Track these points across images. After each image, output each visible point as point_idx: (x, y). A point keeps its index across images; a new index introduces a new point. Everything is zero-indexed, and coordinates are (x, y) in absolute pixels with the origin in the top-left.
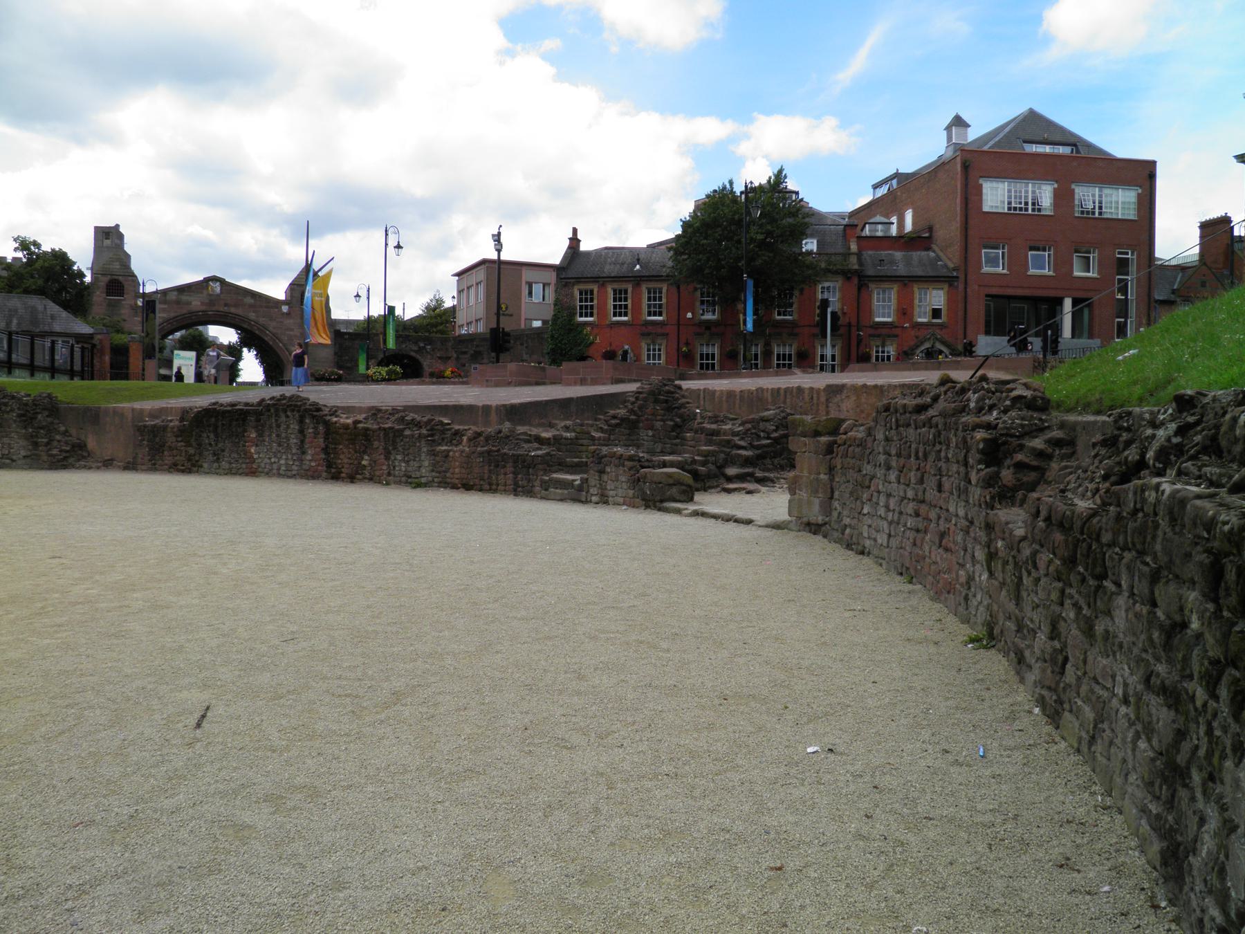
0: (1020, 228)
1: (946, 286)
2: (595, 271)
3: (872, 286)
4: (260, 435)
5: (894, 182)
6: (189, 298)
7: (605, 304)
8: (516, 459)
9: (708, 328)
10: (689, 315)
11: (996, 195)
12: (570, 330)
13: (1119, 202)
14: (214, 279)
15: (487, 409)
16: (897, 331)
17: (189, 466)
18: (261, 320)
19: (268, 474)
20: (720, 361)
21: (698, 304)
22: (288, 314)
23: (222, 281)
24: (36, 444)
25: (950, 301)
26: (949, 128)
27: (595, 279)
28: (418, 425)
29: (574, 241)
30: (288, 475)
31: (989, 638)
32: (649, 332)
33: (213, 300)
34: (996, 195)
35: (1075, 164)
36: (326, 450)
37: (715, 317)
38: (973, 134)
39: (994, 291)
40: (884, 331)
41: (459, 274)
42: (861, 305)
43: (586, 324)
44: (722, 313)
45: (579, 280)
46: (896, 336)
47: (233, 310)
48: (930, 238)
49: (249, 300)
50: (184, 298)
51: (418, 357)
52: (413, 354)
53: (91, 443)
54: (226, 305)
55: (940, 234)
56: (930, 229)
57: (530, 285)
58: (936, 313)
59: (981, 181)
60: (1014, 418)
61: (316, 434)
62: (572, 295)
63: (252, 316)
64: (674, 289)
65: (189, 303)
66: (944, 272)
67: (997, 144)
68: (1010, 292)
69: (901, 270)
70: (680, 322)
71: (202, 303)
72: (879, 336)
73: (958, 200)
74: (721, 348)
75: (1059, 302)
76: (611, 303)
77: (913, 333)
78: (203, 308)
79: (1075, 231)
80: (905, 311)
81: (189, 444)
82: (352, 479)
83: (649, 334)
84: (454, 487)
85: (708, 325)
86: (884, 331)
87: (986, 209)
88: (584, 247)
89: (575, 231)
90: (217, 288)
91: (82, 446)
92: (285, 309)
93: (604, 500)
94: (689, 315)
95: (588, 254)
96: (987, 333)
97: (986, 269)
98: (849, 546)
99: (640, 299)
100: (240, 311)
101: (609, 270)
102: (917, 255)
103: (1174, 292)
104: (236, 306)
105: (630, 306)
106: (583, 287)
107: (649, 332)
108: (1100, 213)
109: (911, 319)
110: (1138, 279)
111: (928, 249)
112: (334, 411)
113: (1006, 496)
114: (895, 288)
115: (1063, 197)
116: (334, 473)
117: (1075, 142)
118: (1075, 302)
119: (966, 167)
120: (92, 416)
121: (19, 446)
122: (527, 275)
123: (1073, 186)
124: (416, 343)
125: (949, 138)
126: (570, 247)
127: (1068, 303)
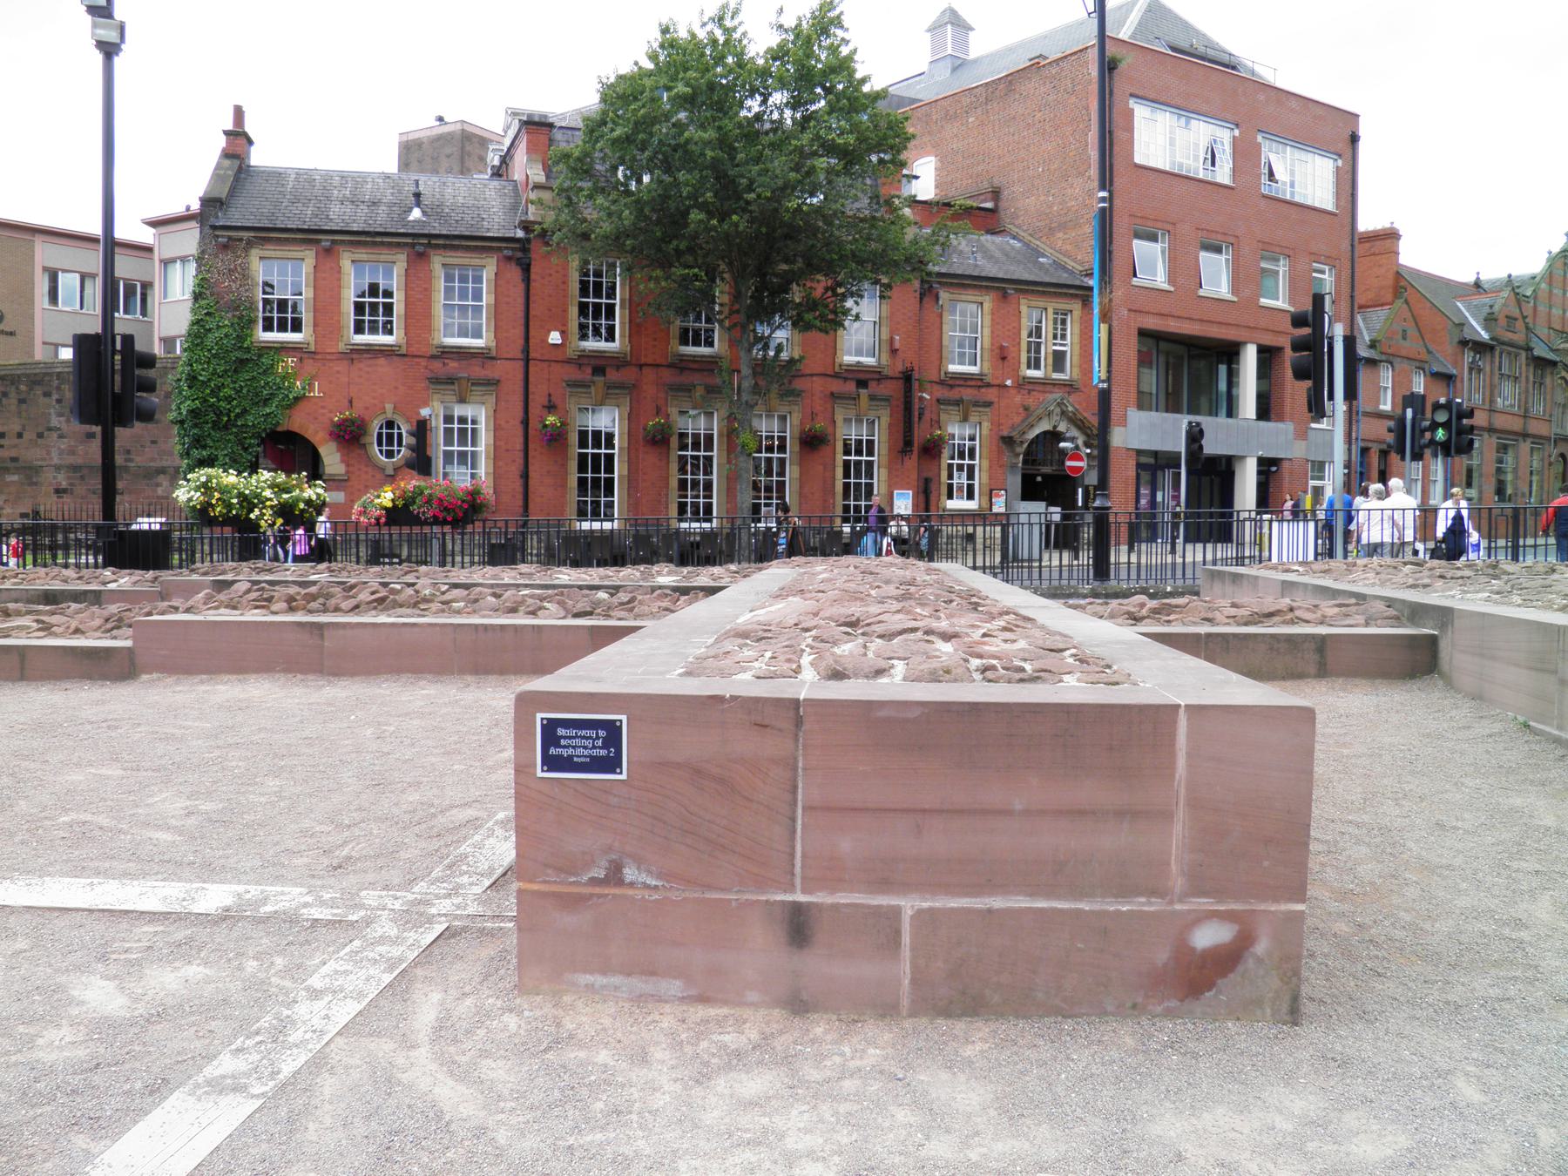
1: (1076, 306)
2: (306, 216)
3: (944, 295)
9: (599, 370)
10: (555, 337)
13: (1306, 177)
16: (991, 394)
21: (574, 311)
26: (935, 28)
27: (308, 236)
29: (238, 138)
32: (454, 372)
35: (1261, 97)
37: (614, 346)
38: (979, 45)
39: (1152, 323)
40: (967, 394)
42: (927, 335)
43: (284, 348)
44: (635, 328)
45: (270, 235)
46: (988, 404)
48: (992, 211)
55: (1024, 204)
56: (996, 194)
57: (53, 277)
59: (1132, 103)
62: (246, 275)
64: (514, 273)
66: (1064, 278)
68: (1173, 326)
69: (992, 270)
72: (957, 403)
73: (1093, 136)
74: (632, 418)
75: (1229, 353)
77: (1018, 399)
80: (1002, 356)
83: (450, 381)
85: (599, 364)
86: (967, 394)
87: (1138, 159)
88: (259, 157)
89: (239, 113)
94: (555, 337)
95: (277, 175)
96: (1140, 407)
99: (428, 292)
101: (339, 215)
102: (987, 239)
103: (1373, 345)
108: (1293, 194)
114: (988, 301)
115: (1245, 155)
119: (1108, 67)
123: (1260, 138)
125: (937, 46)
126: (227, 155)
127: (1250, 357)
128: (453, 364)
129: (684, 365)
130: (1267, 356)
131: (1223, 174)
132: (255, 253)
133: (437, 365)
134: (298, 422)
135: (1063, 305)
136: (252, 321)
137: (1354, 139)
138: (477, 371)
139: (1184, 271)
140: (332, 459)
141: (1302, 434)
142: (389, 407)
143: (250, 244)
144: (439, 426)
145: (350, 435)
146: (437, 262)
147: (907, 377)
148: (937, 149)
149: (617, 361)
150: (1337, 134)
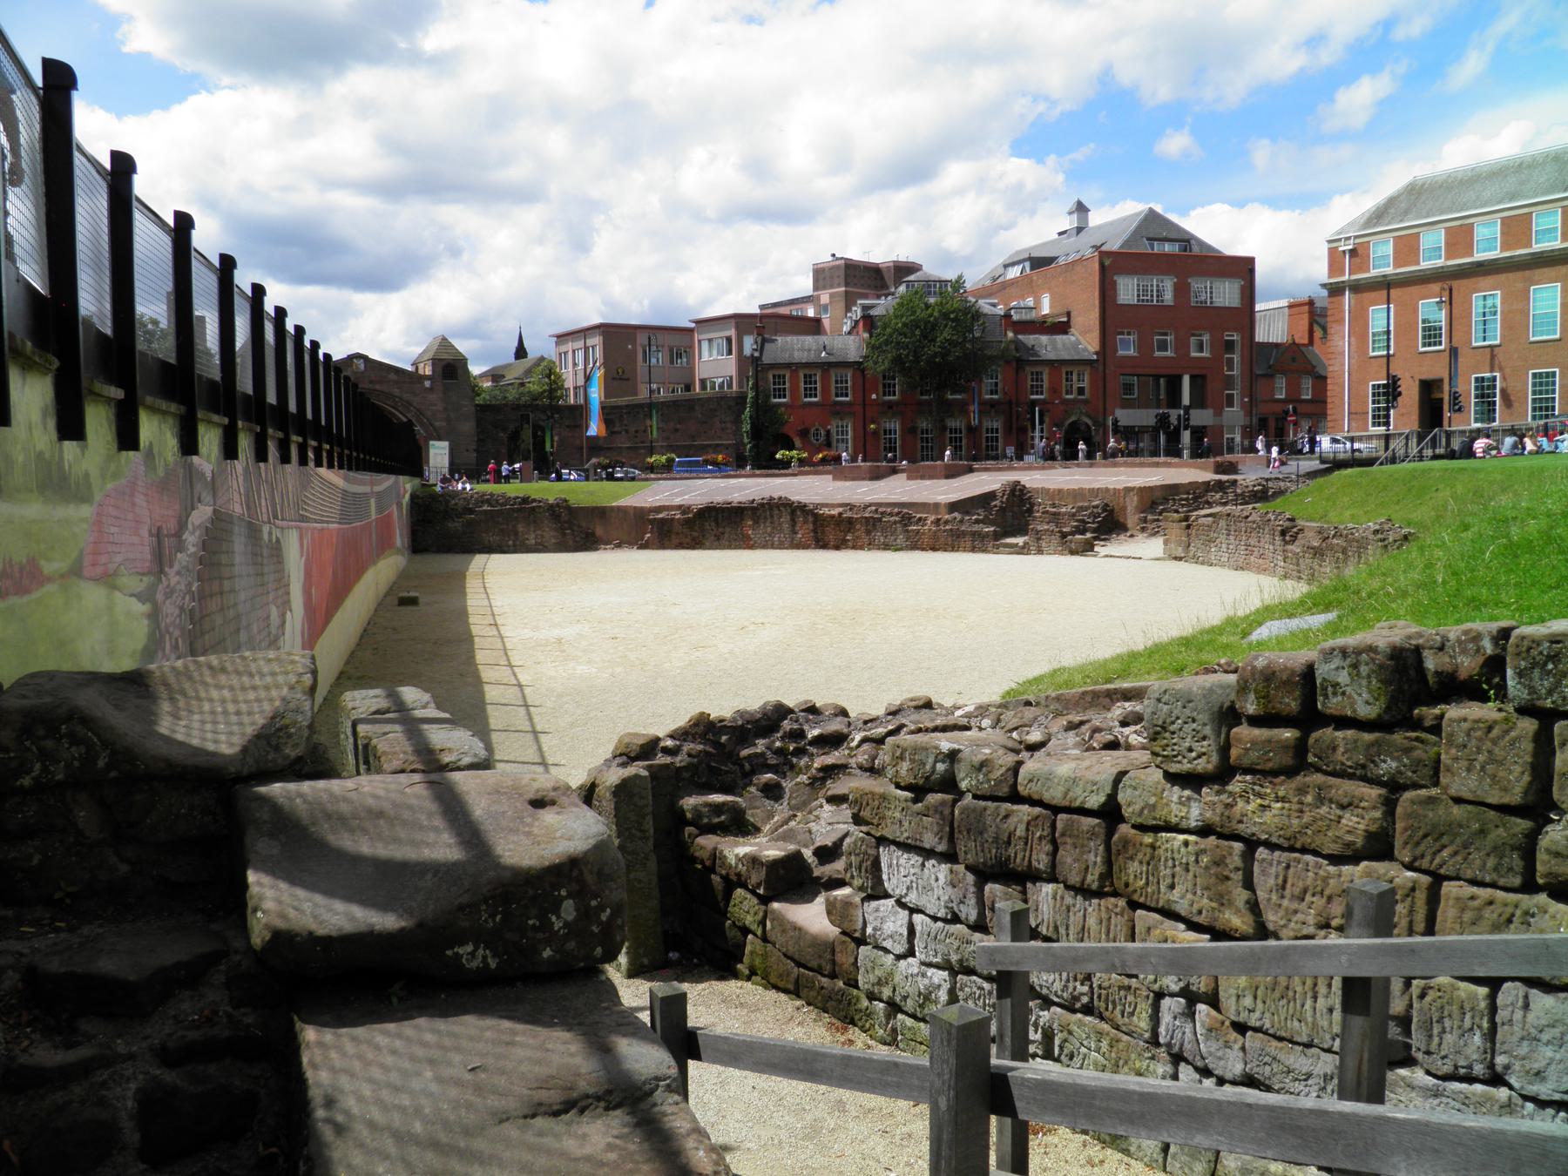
0: (1144, 318)
4: (756, 522)
5: (1027, 264)
7: (798, 386)
8: (973, 534)
11: (1128, 290)
13: (1226, 294)
14: (359, 356)
15: (937, 505)
17: (695, 544)
18: (406, 396)
19: (764, 547)
20: (902, 436)
22: (431, 389)
23: (365, 358)
24: (564, 535)
25: (1093, 382)
27: (788, 366)
28: (891, 514)
30: (781, 546)
31: (1285, 577)
34: (1128, 290)
36: (815, 531)
41: (559, 337)
43: (780, 405)
44: (902, 392)
47: (377, 387)
49: (392, 376)
53: (599, 531)
55: (1077, 321)
56: (1069, 314)
58: (1081, 391)
60: (1287, 524)
61: (805, 522)
63: (396, 392)
67: (1126, 243)
70: (865, 402)
74: (902, 424)
75: (1180, 378)
76: (802, 385)
79: (1188, 316)
80: (1054, 390)
81: (692, 529)
82: (837, 548)
84: (923, 550)
85: (890, 405)
90: (361, 365)
91: (593, 534)
92: (427, 384)
93: (1040, 552)
97: (1121, 353)
98: (1203, 563)
100: (384, 388)
102: (1059, 338)
106: (777, 372)
107: (839, 411)
109: (1060, 397)
110: (1242, 357)
111: (1065, 332)
112: (818, 506)
113: (1286, 543)
115: (1182, 290)
116: (821, 544)
117: (1186, 240)
118: (1192, 378)
119: (1103, 268)
120: (601, 513)
121: (550, 535)
122: (642, 339)
127: (1186, 380)
129: (921, 403)
130: (1198, 381)
131: (1168, 297)
134: (785, 430)
135: (1081, 368)
137: (1252, 271)
139: (1142, 345)
140: (798, 442)
141: (1219, 412)
144: (833, 432)
145: (804, 434)
147: (1010, 403)
148: (1050, 290)
149: (896, 403)
150: (1243, 268)
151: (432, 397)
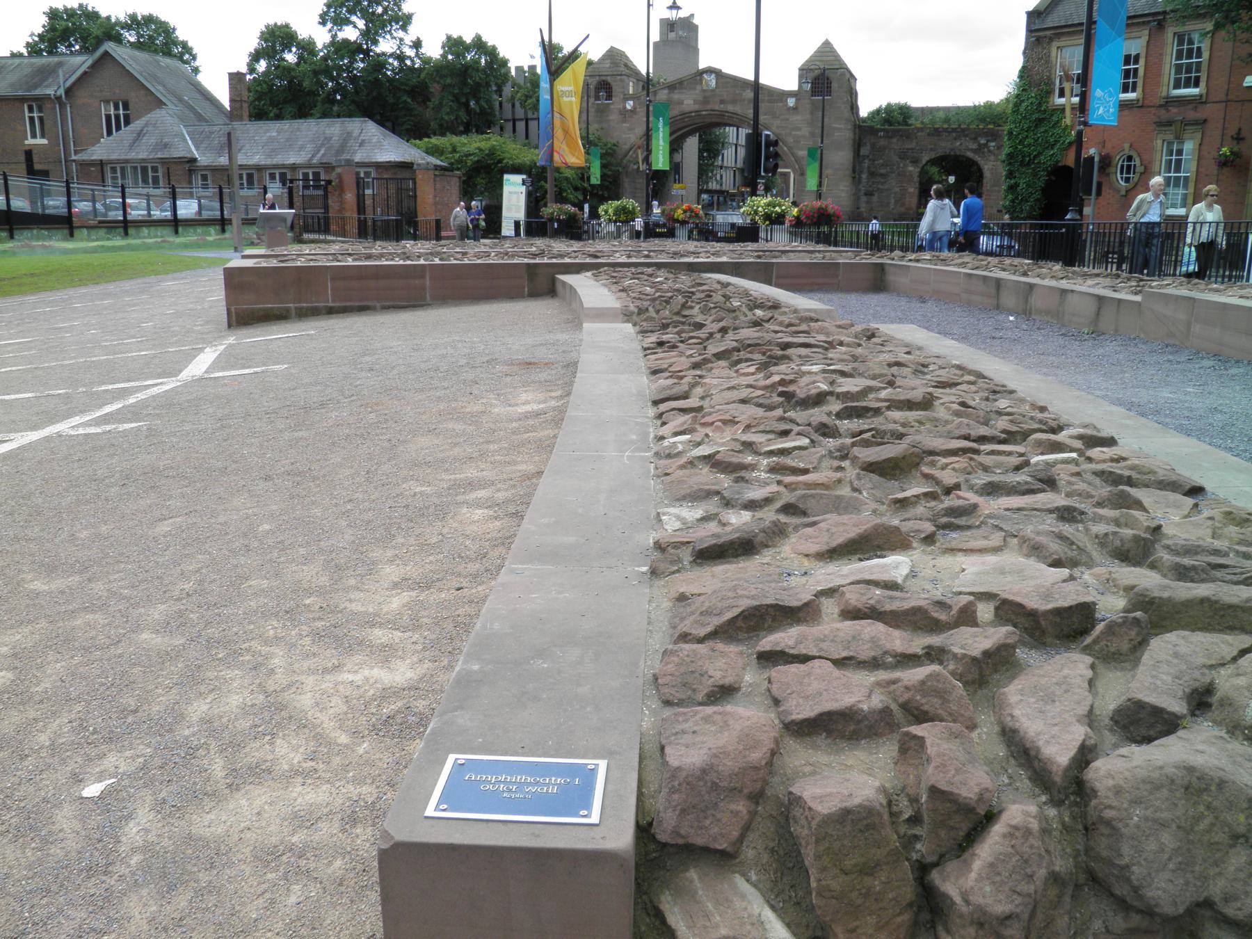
6: (682, 97)
12: (1040, 121)
22: (795, 108)
33: (707, 97)
47: (730, 108)
50: (676, 96)
51: (977, 158)
52: (970, 154)
54: (722, 102)
65: (681, 103)
71: (696, 102)
78: (697, 107)
83: (1169, 123)
90: (712, 81)
92: (791, 102)
99: (1161, 56)
104: (734, 102)
105: (1141, 73)
124: (975, 139)
128: (1174, 110)
132: (1055, 44)
133: (1163, 111)
136: (1049, 93)
138: (1191, 115)
142: (1127, 146)
143: (1051, 40)
146: (1170, 32)
151: (796, 119)
